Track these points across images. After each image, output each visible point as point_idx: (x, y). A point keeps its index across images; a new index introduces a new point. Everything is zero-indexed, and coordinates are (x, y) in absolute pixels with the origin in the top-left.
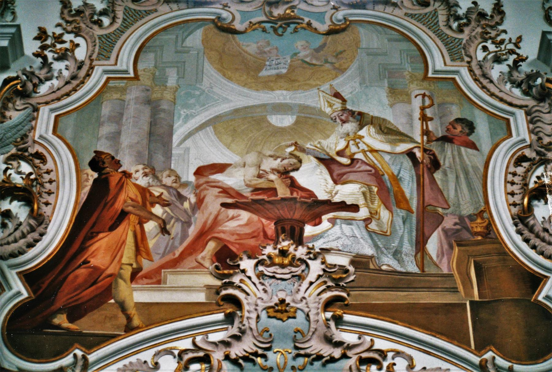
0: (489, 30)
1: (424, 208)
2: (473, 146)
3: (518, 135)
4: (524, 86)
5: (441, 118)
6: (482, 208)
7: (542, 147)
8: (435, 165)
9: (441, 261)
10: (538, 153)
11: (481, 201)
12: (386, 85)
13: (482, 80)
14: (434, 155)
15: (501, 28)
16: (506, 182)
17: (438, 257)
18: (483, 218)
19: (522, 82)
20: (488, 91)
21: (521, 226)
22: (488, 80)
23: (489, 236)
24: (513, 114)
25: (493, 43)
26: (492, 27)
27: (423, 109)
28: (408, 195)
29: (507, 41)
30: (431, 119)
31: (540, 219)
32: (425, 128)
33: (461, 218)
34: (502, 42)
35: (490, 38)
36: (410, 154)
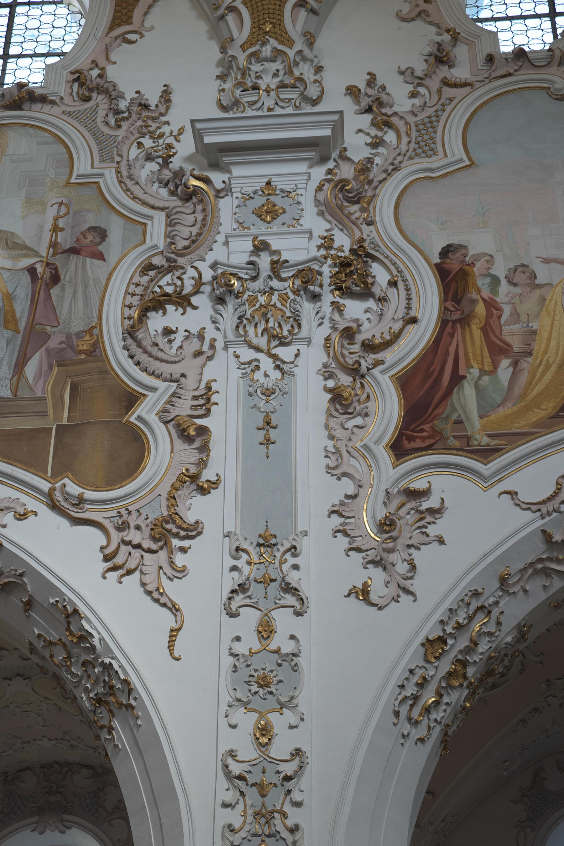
0: (150, 123)
1: (32, 327)
2: (101, 256)
3: (151, 241)
4: (171, 186)
5: (73, 227)
6: (94, 324)
7: (173, 253)
8: (55, 279)
9: (36, 384)
10: (168, 260)
11: (95, 316)
12: (24, 195)
13: (127, 181)
14: (56, 269)
15: (164, 119)
16: (127, 293)
17: (34, 379)
18: (91, 335)
19: (169, 181)
20: (132, 194)
21: (129, 340)
22: (134, 182)
23: (94, 354)
24: (150, 218)
25: (151, 137)
26: (154, 119)
27: (56, 219)
28: (18, 314)
29: (167, 134)
30: (62, 230)
31: (152, 333)
32: (53, 240)
33: (69, 336)
34: (161, 136)
35: (149, 132)
36: (32, 270)
